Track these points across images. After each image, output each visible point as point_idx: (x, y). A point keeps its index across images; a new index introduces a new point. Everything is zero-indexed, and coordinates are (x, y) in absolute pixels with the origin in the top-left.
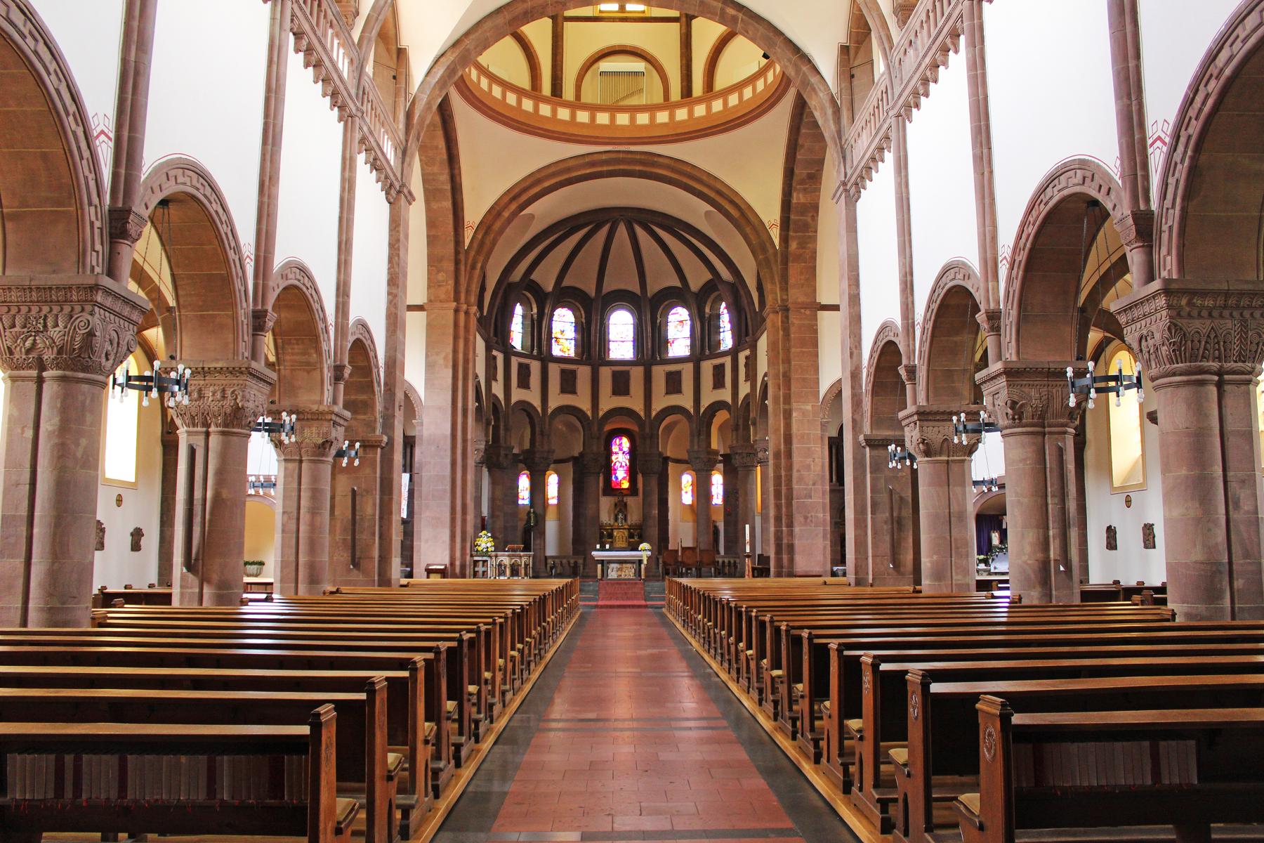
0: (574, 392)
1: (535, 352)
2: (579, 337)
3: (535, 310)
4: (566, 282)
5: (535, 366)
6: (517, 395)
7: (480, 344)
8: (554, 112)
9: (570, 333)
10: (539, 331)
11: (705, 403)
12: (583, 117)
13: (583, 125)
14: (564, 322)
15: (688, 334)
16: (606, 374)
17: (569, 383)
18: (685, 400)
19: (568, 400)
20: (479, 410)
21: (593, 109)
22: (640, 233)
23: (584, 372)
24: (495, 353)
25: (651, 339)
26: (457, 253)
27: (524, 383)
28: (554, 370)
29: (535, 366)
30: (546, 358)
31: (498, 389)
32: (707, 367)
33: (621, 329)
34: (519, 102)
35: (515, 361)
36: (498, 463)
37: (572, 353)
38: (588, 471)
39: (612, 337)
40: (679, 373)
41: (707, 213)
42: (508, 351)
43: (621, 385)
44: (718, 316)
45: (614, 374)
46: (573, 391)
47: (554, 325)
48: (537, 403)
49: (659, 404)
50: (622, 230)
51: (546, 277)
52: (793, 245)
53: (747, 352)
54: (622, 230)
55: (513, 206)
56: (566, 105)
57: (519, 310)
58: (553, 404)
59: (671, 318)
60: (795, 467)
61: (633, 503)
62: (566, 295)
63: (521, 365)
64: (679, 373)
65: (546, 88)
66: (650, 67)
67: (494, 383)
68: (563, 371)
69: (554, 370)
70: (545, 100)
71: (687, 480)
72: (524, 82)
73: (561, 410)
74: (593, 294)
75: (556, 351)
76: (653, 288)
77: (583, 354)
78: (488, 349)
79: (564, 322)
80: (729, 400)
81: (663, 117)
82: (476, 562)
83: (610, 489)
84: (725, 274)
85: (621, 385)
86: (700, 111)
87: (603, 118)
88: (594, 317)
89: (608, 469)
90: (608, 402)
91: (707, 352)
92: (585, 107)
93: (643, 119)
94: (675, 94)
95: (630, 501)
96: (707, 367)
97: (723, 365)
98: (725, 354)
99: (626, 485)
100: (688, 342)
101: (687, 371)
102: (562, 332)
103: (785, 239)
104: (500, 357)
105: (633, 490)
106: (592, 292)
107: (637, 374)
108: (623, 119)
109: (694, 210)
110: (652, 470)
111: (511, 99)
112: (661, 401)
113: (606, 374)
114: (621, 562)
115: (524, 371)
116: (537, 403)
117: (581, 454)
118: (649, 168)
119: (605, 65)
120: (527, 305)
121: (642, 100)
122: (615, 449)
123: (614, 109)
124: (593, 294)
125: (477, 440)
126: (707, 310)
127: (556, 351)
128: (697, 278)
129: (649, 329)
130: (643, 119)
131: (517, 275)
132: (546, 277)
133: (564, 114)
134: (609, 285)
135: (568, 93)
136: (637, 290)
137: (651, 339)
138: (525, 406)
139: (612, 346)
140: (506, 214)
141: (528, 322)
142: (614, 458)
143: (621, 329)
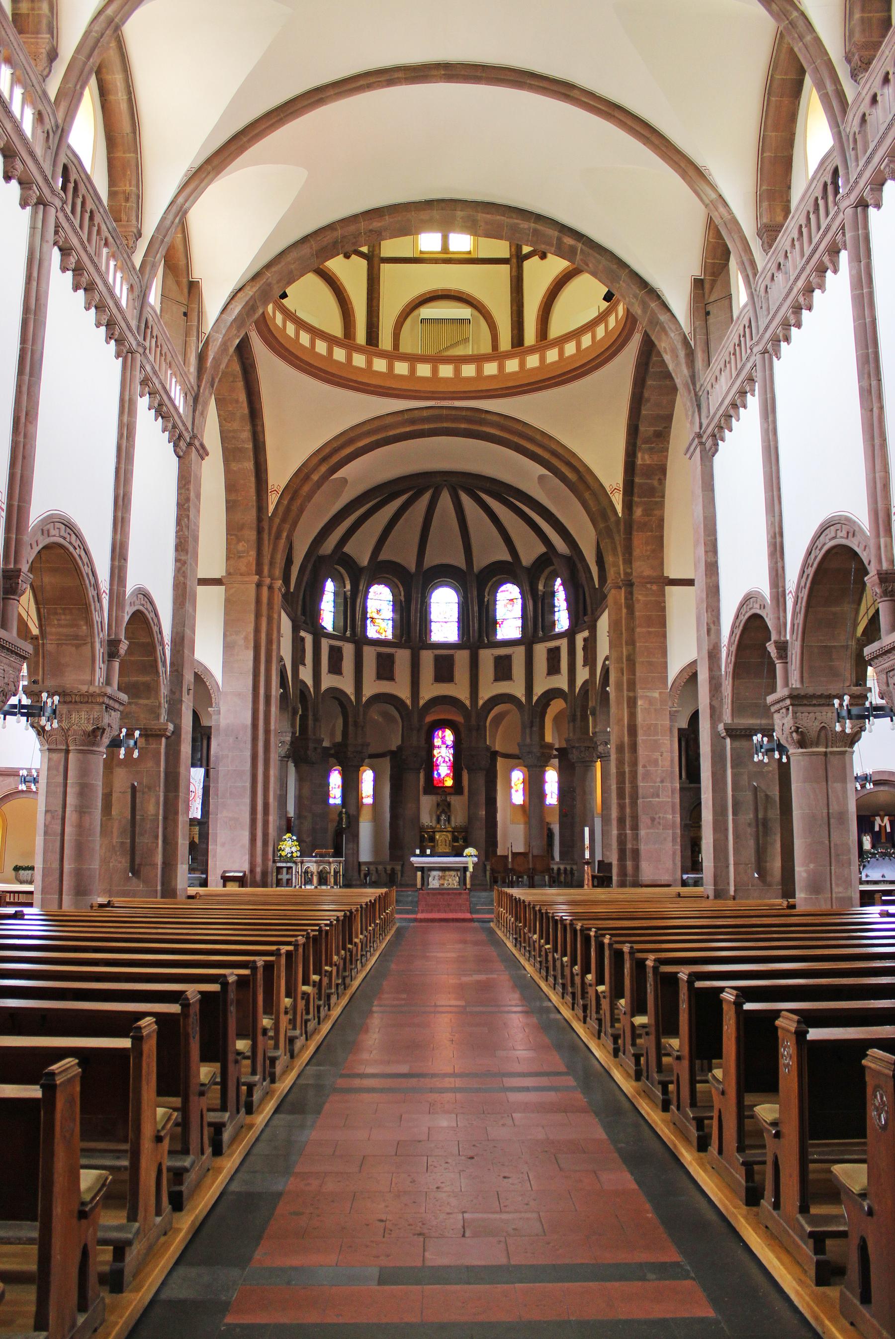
0: (391, 678)
1: (348, 633)
2: (398, 617)
3: (348, 587)
4: (382, 557)
5: (348, 649)
6: (328, 681)
7: (286, 624)
8: (369, 363)
9: (388, 612)
10: (353, 610)
11: (539, 690)
12: (401, 368)
13: (401, 377)
14: (380, 601)
15: (519, 614)
16: (427, 658)
17: (385, 669)
19: (385, 687)
20: (284, 698)
21: (413, 359)
23: (402, 657)
24: (303, 634)
25: (477, 619)
26: (260, 520)
27: (336, 668)
28: (370, 655)
29: (348, 649)
30: (360, 640)
31: (306, 674)
32: (541, 650)
33: (444, 610)
34: (330, 351)
35: (325, 644)
36: (307, 757)
37: (389, 635)
38: (407, 768)
39: (434, 616)
40: (508, 658)
41: (541, 478)
42: (318, 632)
43: (444, 670)
44: (553, 594)
45: (437, 659)
46: (391, 678)
48: (350, 690)
49: (487, 691)
50: (445, 500)
51: (361, 550)
52: (638, 512)
53: (586, 634)
54: (445, 499)
55: (323, 469)
56: (383, 355)
57: (330, 586)
58: (368, 691)
59: (500, 596)
60: (641, 761)
61: (458, 803)
64: (508, 658)
65: (361, 337)
66: (476, 313)
67: (301, 668)
68: (379, 656)
69: (370, 655)
70: (359, 349)
71: (517, 776)
72: (336, 328)
73: (377, 698)
74: (413, 568)
75: (372, 633)
76: (481, 561)
78: (296, 629)
79: (380, 601)
80: (565, 687)
81: (490, 369)
82: (279, 869)
83: (432, 787)
84: (561, 546)
85: (444, 670)
86: (533, 361)
87: (424, 370)
88: (414, 595)
89: (430, 765)
90: (430, 690)
91: (541, 634)
92: (404, 358)
93: (468, 371)
94: (505, 343)
95: (454, 800)
96: (541, 650)
97: (558, 649)
98: (560, 636)
99: (449, 782)
100: (519, 623)
101: (518, 654)
102: (378, 611)
103: (628, 505)
104: (309, 639)
105: (457, 788)
107: (462, 658)
108: (446, 371)
109: (525, 474)
110: (478, 766)
111: (321, 347)
113: (427, 658)
114: (444, 869)
115: (336, 655)
116: (350, 690)
117: (400, 748)
118: (475, 426)
119: (426, 312)
120: (339, 580)
121: (468, 350)
122: (438, 742)
123: (436, 360)
124: (413, 568)
125: (281, 733)
126: (541, 587)
127: (372, 633)
128: (530, 550)
129: (476, 608)
130: (468, 371)
131: (329, 546)
132: (361, 550)
133: (380, 365)
134: (432, 559)
135: (386, 342)
137: (477, 619)
138: (336, 694)
139: (434, 626)
140: (315, 477)
142: (436, 752)
143: (444, 610)
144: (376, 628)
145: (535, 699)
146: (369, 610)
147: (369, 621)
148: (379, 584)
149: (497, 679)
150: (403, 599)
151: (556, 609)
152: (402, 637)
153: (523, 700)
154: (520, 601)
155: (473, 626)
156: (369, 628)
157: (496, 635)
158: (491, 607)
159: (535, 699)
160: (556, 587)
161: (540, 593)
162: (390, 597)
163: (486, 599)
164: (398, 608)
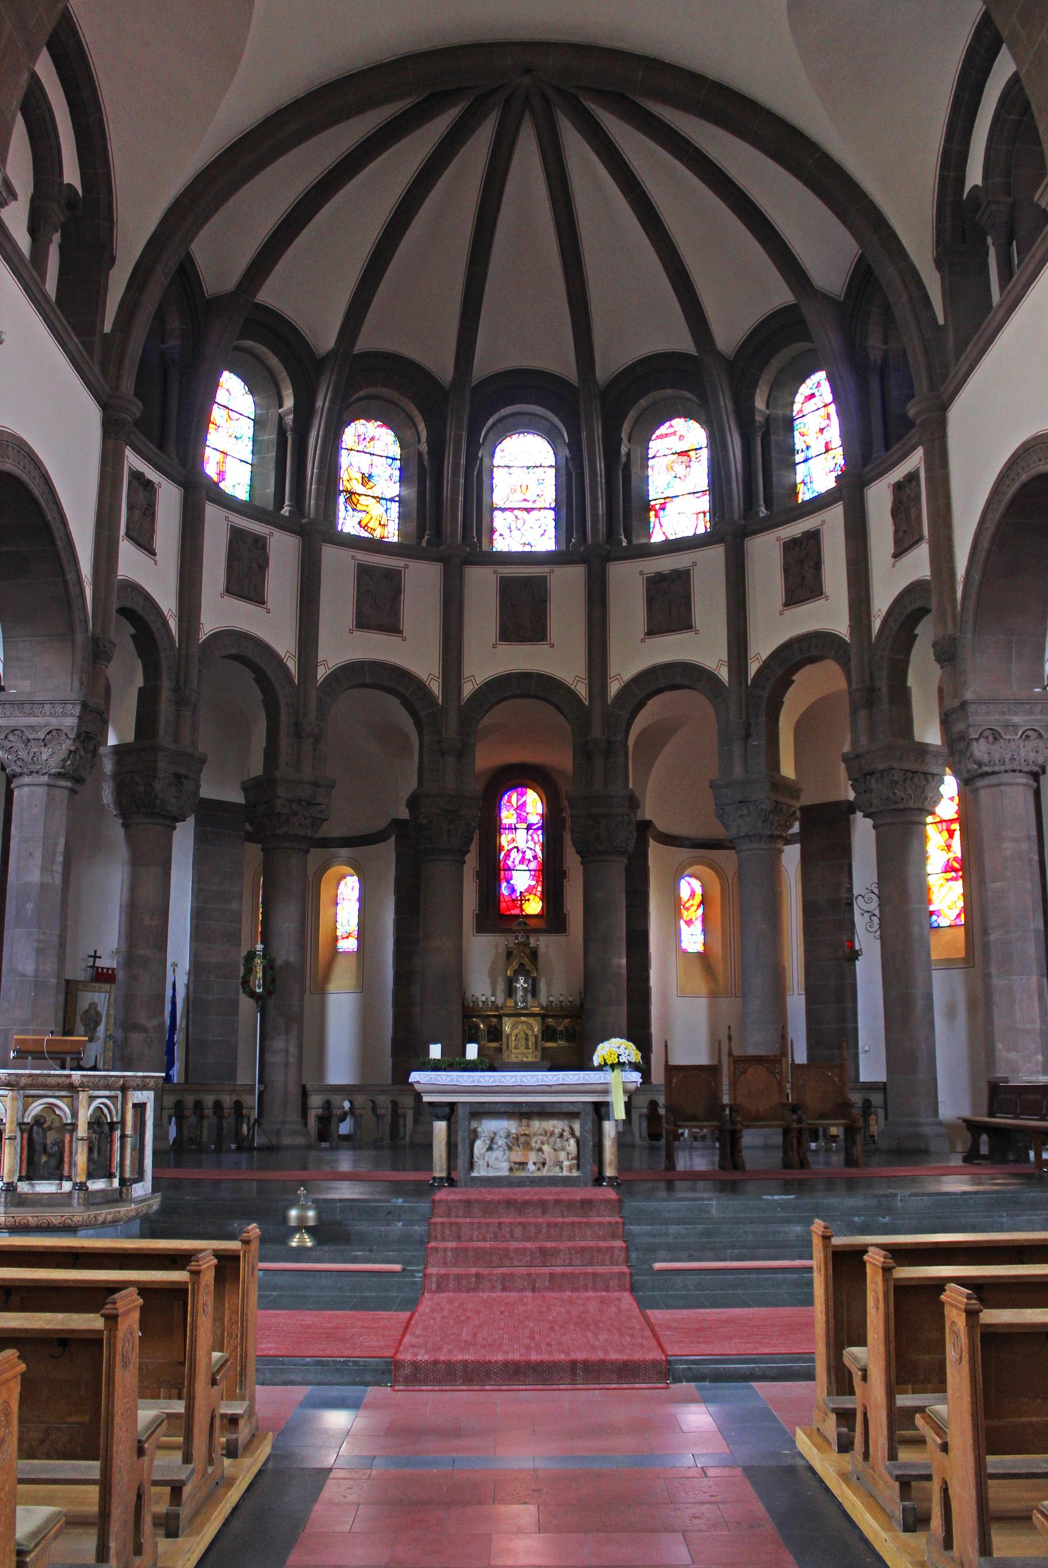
0: (392, 627)
1: (286, 511)
2: (411, 493)
3: (289, 403)
9: (388, 483)
10: (299, 461)
11: (762, 648)
14: (371, 460)
15: (703, 484)
17: (378, 601)
18: (705, 647)
22: (578, 151)
25: (603, 502)
30: (315, 531)
33: (523, 483)
37: (392, 534)
39: (499, 498)
40: (682, 577)
45: (506, 586)
46: (392, 627)
47: (345, 459)
49: (626, 664)
59: (655, 446)
62: (375, 381)
63: (237, 536)
64: (682, 577)
68: (364, 572)
69: (338, 572)
76: (612, 358)
77: (421, 532)
88: (450, 433)
90: (488, 659)
91: (763, 512)
96: (766, 552)
97: (813, 537)
100: (704, 503)
102: (367, 479)
104: (169, 498)
106: (442, 365)
107: (567, 586)
112: (633, 655)
113: (481, 587)
116: (284, 644)
120: (258, 382)
126: (760, 404)
129: (600, 466)
132: (312, 293)
136: (570, 371)
137: (603, 502)
138: (245, 652)
139: (500, 520)
141: (270, 436)
143: (523, 483)
144: (358, 516)
145: (753, 668)
146: (344, 475)
147: (342, 499)
148: (368, 420)
149: (652, 631)
150: (424, 447)
151: (799, 458)
152: (420, 537)
153: (724, 674)
154: (704, 454)
155: (594, 508)
156: (342, 514)
157: (650, 536)
158: (635, 470)
159: (753, 668)
160: (796, 407)
161: (759, 418)
162: (396, 451)
163: (624, 450)
164: (413, 470)
